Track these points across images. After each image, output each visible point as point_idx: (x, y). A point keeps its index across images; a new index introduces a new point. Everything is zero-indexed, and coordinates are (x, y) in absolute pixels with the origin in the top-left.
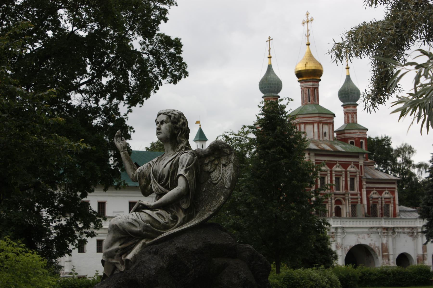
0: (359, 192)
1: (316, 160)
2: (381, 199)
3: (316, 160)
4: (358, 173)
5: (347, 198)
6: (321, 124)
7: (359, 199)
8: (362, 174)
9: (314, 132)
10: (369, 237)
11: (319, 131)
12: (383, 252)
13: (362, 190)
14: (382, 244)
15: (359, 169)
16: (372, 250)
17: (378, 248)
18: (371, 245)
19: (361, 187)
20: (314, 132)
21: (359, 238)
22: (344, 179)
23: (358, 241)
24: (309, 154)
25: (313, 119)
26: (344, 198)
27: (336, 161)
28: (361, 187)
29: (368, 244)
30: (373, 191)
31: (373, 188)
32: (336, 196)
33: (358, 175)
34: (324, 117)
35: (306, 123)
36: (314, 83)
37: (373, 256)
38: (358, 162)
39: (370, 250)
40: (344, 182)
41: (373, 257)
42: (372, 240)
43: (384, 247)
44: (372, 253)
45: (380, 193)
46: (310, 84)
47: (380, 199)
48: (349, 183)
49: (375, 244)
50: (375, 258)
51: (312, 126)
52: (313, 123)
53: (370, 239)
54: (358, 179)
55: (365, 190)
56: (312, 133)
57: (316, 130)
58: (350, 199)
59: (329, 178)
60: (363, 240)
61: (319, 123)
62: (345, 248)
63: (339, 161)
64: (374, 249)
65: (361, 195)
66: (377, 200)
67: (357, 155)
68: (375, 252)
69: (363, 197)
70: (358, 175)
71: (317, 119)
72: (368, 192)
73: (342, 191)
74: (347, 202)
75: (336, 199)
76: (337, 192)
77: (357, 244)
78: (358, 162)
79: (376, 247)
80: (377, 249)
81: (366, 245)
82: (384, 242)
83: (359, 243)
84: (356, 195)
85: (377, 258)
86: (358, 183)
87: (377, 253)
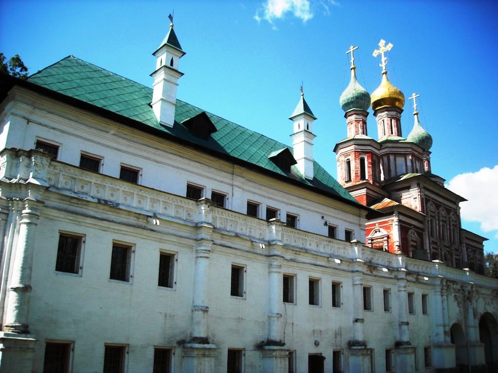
9: (406, 165)
11: (412, 166)
19: (461, 243)
20: (406, 165)
25: (405, 150)
26: (449, 252)
28: (461, 243)
35: (396, 155)
51: (403, 159)
52: (405, 155)
55: (464, 245)
56: (404, 168)
57: (409, 164)
61: (413, 155)
67: (454, 200)
71: (410, 150)
73: (447, 243)
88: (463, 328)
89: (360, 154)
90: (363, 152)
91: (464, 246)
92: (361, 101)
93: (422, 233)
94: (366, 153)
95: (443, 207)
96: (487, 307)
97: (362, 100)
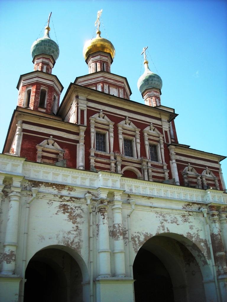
0: (164, 163)
1: (87, 106)
2: (201, 178)
3: (87, 106)
4: (161, 138)
5: (144, 167)
6: (107, 85)
7: (167, 174)
8: (167, 141)
10: (186, 221)
12: (215, 252)
13: (171, 162)
14: (213, 236)
15: (162, 133)
16: (195, 246)
17: (205, 242)
18: (192, 237)
19: (168, 159)
21: (166, 221)
22: (138, 141)
23: (163, 227)
24: (77, 97)
26: (140, 169)
27: (125, 117)
28: (168, 159)
29: (185, 235)
30: (187, 166)
31: (187, 163)
32: (126, 163)
33: (162, 141)
34: (111, 79)
36: (101, 56)
37: (198, 259)
38: (161, 126)
39: (189, 248)
40: (139, 146)
41: (197, 264)
42: (191, 227)
43: (216, 242)
44: (195, 254)
45: (200, 171)
46: (98, 57)
47: (199, 178)
48: (147, 148)
49: (198, 236)
50: (201, 264)
53: (187, 224)
54: (162, 146)
55: (174, 161)
58: (150, 171)
59: (112, 134)
60: (175, 224)
62: (133, 239)
63: (129, 117)
64: (197, 244)
65: (169, 167)
66: (195, 180)
68: (199, 251)
69: (172, 172)
70: (162, 141)
72: (180, 168)
73: (135, 159)
74: (146, 173)
75: (125, 168)
76: (127, 158)
77: (161, 232)
78: (161, 126)
79: (201, 241)
80: (202, 244)
81: (182, 236)
82: (216, 231)
83: (166, 231)
84: (162, 167)
85: (205, 263)
86: (163, 151)
87: (205, 254)
88: (84, 253)
89: (27, 88)
90: (29, 85)
91: (172, 163)
92: (41, 47)
93: (76, 146)
94: (32, 84)
95: (129, 120)
96: (166, 225)
97: (42, 45)
